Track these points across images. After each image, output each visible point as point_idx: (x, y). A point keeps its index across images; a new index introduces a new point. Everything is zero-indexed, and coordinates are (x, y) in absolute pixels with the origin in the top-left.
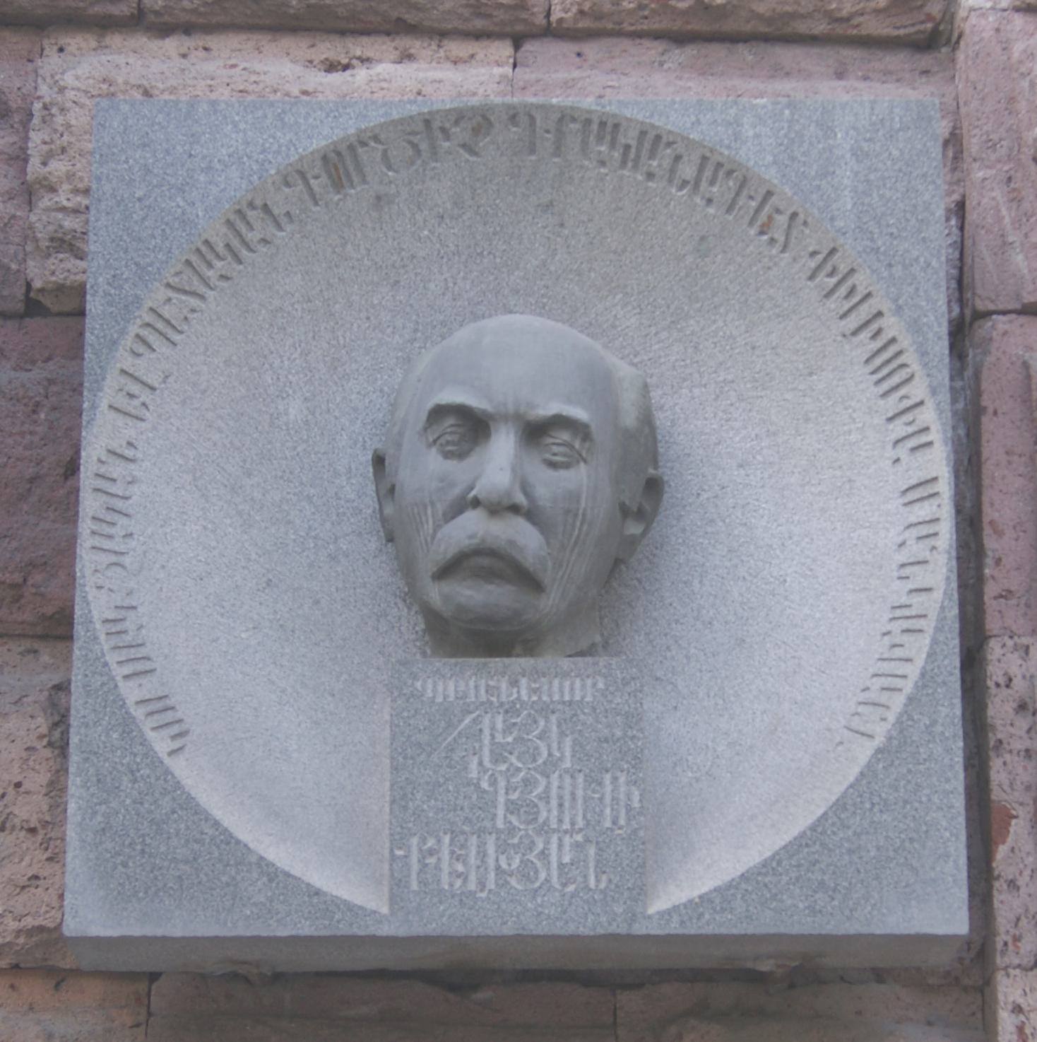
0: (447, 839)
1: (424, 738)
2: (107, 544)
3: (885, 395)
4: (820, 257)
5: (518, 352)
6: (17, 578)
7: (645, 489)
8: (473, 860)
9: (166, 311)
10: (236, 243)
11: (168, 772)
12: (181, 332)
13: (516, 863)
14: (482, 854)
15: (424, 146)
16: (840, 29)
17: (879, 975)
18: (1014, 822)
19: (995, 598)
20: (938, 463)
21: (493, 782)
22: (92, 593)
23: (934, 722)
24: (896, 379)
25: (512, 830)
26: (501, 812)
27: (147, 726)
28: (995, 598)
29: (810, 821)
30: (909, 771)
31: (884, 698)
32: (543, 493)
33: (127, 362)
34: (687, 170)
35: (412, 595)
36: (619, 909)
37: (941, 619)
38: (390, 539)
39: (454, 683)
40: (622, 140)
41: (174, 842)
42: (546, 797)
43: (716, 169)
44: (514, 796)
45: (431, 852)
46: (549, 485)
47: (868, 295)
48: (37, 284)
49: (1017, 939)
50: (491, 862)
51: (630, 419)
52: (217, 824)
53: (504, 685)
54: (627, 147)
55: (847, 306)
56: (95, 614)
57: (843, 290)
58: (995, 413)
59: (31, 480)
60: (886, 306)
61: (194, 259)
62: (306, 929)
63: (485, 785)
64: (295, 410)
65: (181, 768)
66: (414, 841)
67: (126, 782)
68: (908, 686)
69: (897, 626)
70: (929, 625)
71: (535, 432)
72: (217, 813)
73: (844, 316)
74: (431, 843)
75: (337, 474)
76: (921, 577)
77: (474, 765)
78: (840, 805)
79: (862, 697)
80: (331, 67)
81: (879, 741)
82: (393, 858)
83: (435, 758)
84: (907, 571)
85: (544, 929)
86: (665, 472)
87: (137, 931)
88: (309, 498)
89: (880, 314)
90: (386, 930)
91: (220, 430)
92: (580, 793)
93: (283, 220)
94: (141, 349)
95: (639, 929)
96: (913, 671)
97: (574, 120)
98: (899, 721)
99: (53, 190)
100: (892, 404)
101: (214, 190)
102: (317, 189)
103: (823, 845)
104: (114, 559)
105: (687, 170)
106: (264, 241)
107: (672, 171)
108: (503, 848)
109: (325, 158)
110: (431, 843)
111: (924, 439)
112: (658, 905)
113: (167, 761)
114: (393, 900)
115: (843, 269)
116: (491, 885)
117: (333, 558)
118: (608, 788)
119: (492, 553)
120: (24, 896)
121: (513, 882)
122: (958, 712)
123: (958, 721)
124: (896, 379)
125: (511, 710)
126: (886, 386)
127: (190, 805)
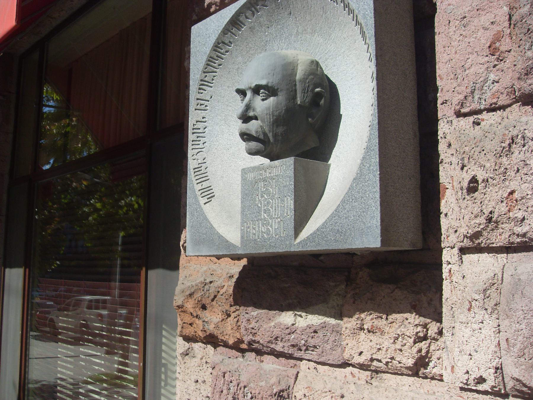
8: (257, 230)
9: (206, 79)
12: (212, 83)
14: (259, 227)
15: (253, 9)
18: (447, 190)
19: (442, 104)
28: (442, 104)
30: (363, 185)
58: (439, 34)
82: (241, 230)
91: (230, 106)
94: (202, 91)
102: (234, 32)
103: (339, 216)
104: (200, 150)
109: (231, 23)
121: (265, 235)
122: (378, 160)
123: (378, 164)
125: (264, 180)
127: (206, 219)
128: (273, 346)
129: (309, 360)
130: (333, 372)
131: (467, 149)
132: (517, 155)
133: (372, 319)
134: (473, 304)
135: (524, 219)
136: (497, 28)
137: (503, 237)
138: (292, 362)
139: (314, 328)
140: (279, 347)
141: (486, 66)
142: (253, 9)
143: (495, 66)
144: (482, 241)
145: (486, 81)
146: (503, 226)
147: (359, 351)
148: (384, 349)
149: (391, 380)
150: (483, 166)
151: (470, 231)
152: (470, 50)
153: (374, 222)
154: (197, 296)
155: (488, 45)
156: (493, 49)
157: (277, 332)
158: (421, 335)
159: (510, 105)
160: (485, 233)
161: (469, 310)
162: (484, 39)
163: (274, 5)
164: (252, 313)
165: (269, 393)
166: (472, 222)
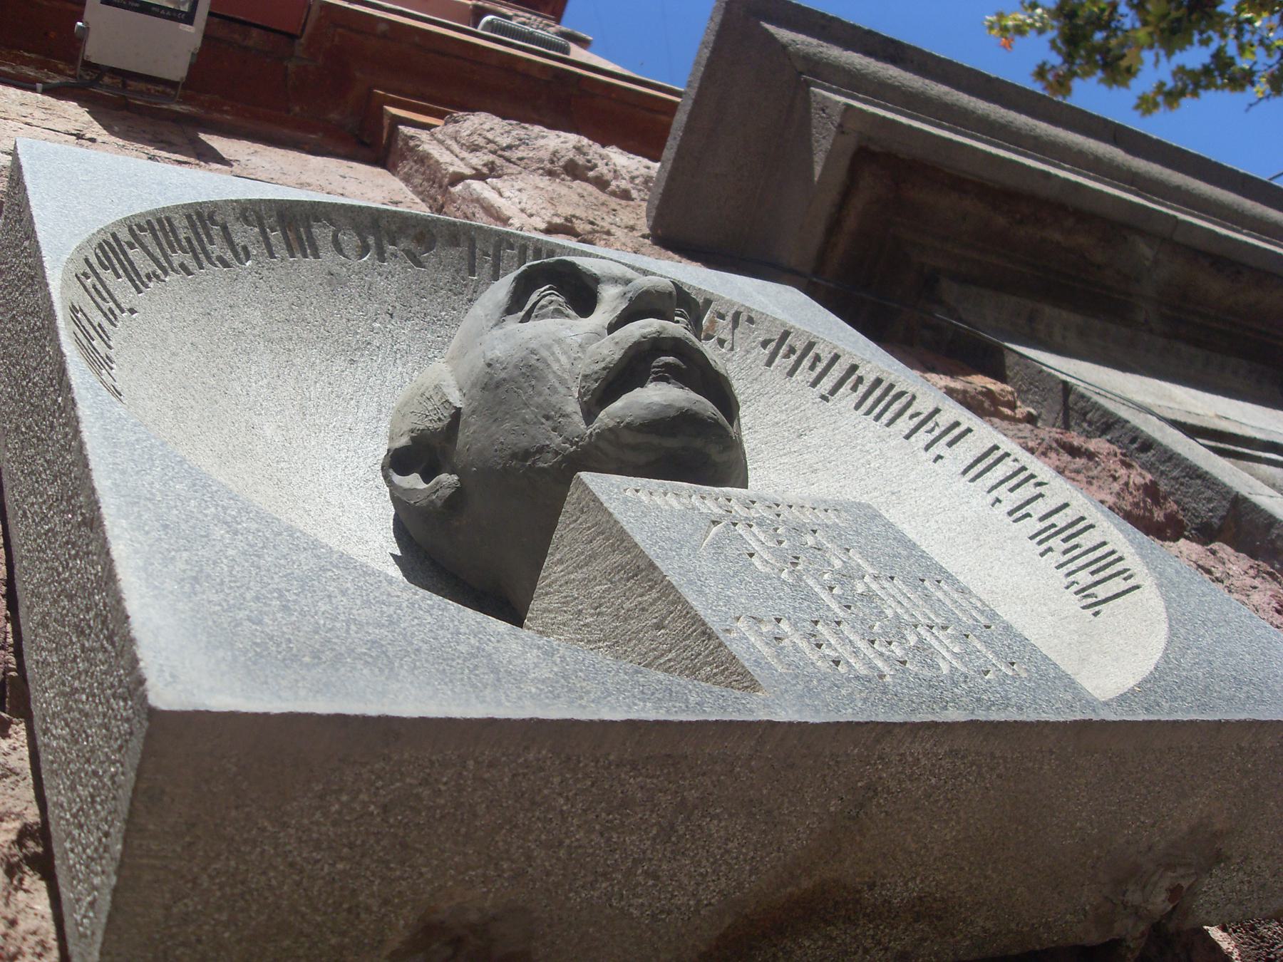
4: (772, 346)
15: (371, 241)
55: (814, 374)
97: (511, 247)
102: (273, 241)
115: (800, 346)
124: (896, 406)
142: (371, 241)
163: (447, 276)
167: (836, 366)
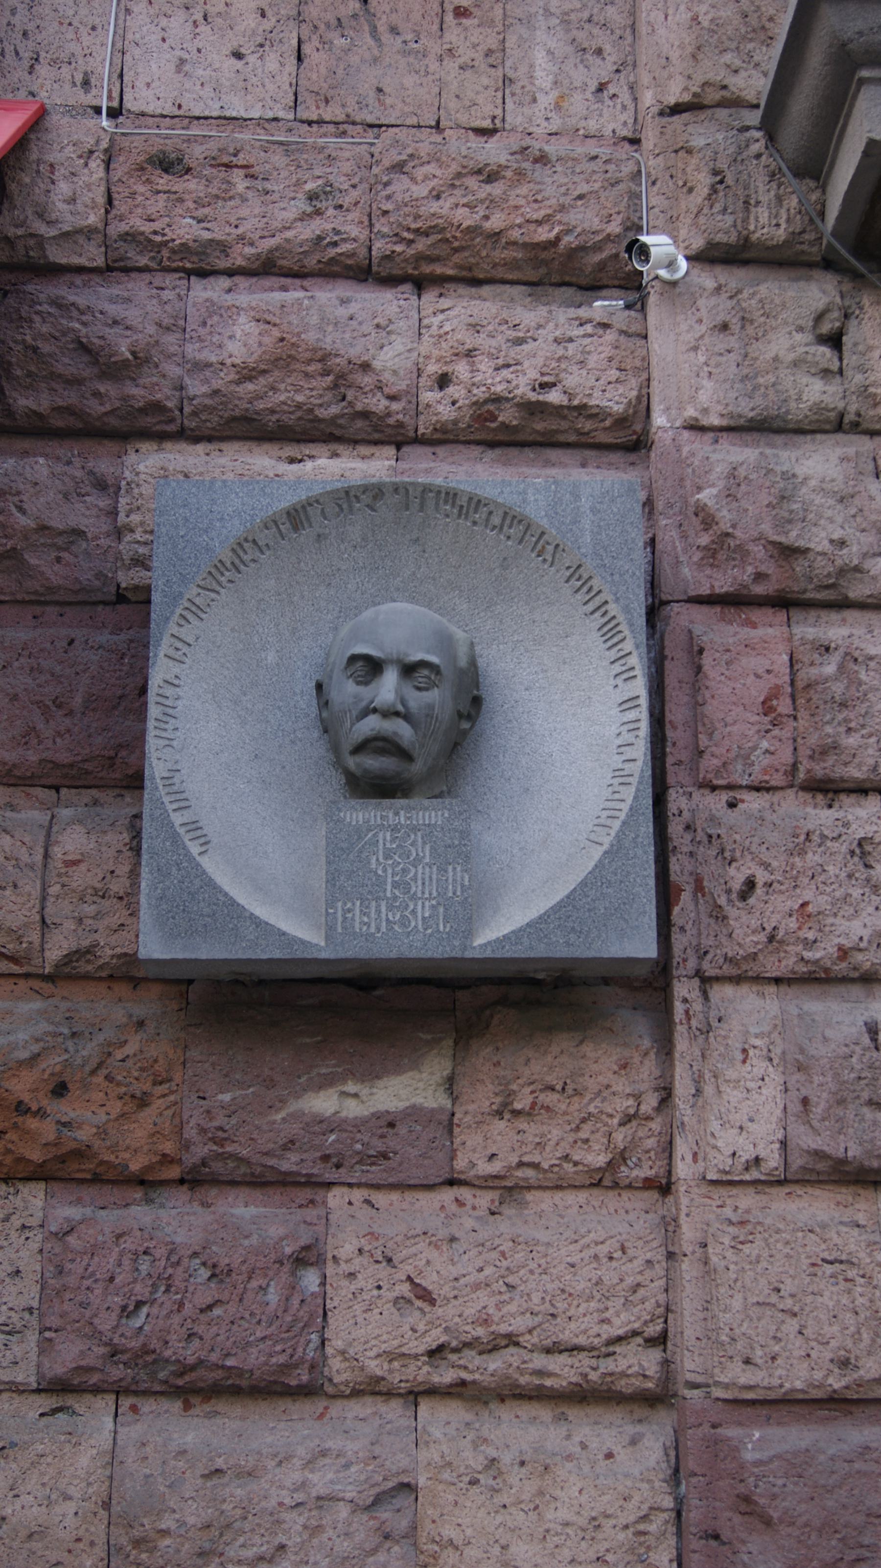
0: (358, 903)
1: (345, 845)
2: (164, 734)
3: (609, 648)
5: (399, 624)
6: (112, 753)
7: (472, 701)
9: (197, 601)
10: (237, 562)
11: (198, 865)
13: (398, 917)
14: (378, 912)
15: (345, 506)
16: (583, 439)
17: (606, 981)
20: (640, 688)
21: (385, 871)
22: (155, 762)
23: (637, 836)
24: (615, 640)
25: (395, 898)
26: (389, 887)
27: (186, 839)
29: (566, 892)
31: (609, 822)
32: (413, 705)
33: (175, 630)
34: (496, 520)
35: (338, 763)
36: (457, 943)
37: (641, 777)
38: (326, 731)
39: (362, 814)
40: (458, 502)
41: (202, 904)
42: (415, 879)
43: (512, 519)
44: (397, 878)
45: (349, 911)
46: (417, 700)
47: (600, 592)
48: (123, 585)
49: (685, 960)
50: (383, 916)
51: (463, 662)
52: (226, 895)
53: (391, 815)
54: (462, 507)
56: (157, 775)
57: (585, 589)
59: (120, 698)
60: (610, 598)
61: (213, 570)
62: (277, 955)
63: (380, 872)
64: (271, 657)
65: (206, 863)
66: (340, 904)
67: (174, 870)
68: (623, 816)
69: (616, 781)
70: (634, 780)
71: (409, 670)
72: (226, 888)
73: (585, 603)
74: (349, 905)
75: (295, 694)
76: (629, 753)
77: (374, 861)
78: (583, 884)
79: (597, 821)
80: (292, 461)
81: (606, 847)
82: (327, 914)
83: (351, 856)
84: (622, 749)
85: (414, 954)
86: (484, 693)
87: (180, 956)
88: (279, 708)
89: (606, 602)
90: (324, 955)
92: (434, 877)
93: (264, 549)
94: (183, 622)
95: (469, 954)
96: (625, 807)
98: (617, 836)
99: (132, 531)
100: (613, 654)
101: (225, 531)
105: (496, 520)
106: (254, 561)
107: (487, 520)
108: (390, 908)
109: (288, 513)
110: (349, 905)
111: (632, 674)
112: (479, 941)
113: (198, 858)
114: (327, 938)
115: (585, 576)
116: (384, 929)
117: (293, 742)
118: (451, 874)
119: (384, 739)
120: (116, 936)
121: (396, 927)
123: (651, 835)
124: (615, 640)
125: (395, 829)
126: (610, 643)
128: (272, 1162)
129: (350, 1185)
130: (412, 1204)
131: (737, 837)
132: (813, 858)
133: (532, 1092)
134: (751, 1052)
135: (815, 941)
136: (773, 680)
137: (784, 963)
138: (304, 1194)
139: (390, 1118)
140: (289, 1163)
141: (756, 728)
143: (767, 731)
144: (754, 969)
145: (755, 748)
146: (789, 948)
147: (489, 1152)
148: (552, 1143)
149: (544, 1201)
150: (766, 866)
151: (741, 952)
152: (734, 699)
153: (646, 919)
154: (53, 1062)
155: (762, 699)
156: (767, 708)
157: (295, 1129)
158: (632, 1111)
159: (782, 788)
160: (761, 957)
161: (744, 1061)
162: (757, 691)
164: (220, 1097)
165: (273, 1256)
166: (748, 940)
167: (598, 598)
